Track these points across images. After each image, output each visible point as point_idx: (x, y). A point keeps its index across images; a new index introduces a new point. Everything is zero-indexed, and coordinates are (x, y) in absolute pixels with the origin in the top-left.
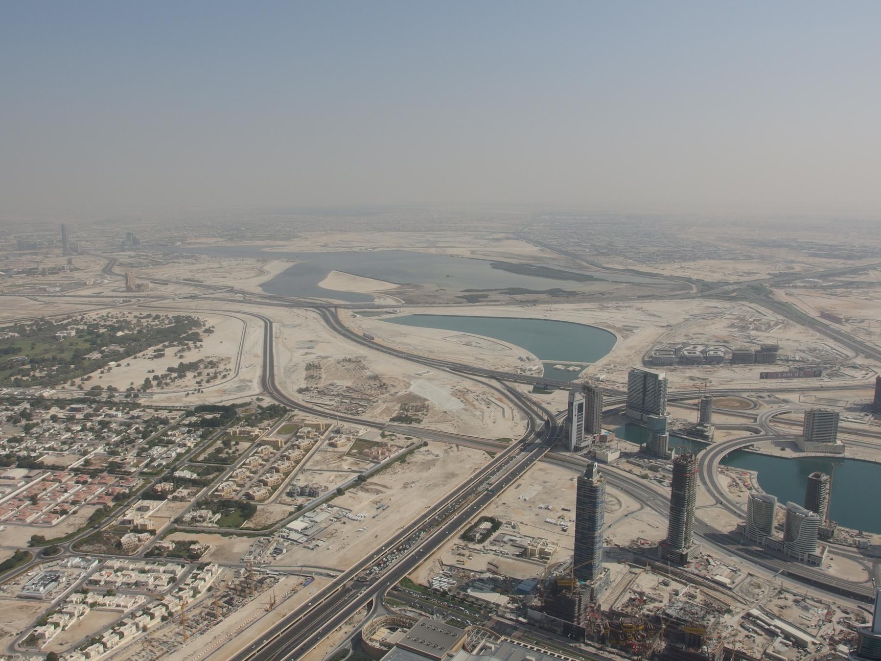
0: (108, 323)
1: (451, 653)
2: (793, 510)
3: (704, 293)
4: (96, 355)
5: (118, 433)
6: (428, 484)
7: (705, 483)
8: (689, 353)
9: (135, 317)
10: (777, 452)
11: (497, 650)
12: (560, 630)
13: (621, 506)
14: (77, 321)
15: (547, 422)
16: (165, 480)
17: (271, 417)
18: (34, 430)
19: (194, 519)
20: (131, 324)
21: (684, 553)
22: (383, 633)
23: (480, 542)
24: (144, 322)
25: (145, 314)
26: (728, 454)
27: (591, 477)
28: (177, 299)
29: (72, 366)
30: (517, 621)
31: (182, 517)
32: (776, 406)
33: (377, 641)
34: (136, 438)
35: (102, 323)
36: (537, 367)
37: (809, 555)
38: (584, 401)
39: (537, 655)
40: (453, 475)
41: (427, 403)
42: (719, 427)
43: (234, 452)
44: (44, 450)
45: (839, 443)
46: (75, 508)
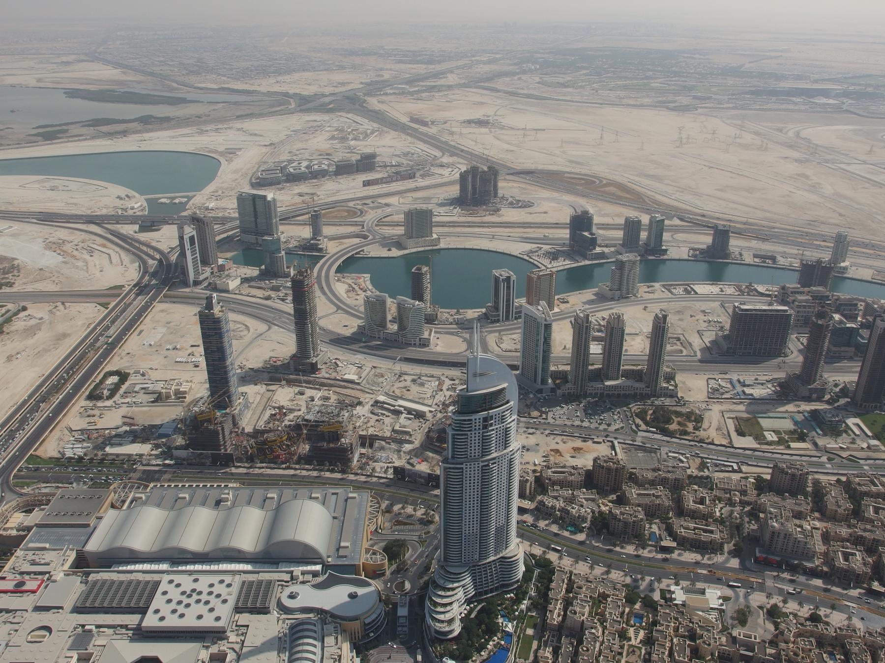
1: (99, 515)
2: (402, 303)
3: (303, 107)
6: (36, 351)
7: (324, 293)
8: (294, 170)
10: (384, 253)
11: (148, 498)
12: (208, 462)
13: (249, 331)
15: (160, 261)
21: (314, 362)
22: (18, 519)
23: (110, 397)
26: (343, 262)
27: (212, 309)
30: (165, 465)
32: (379, 211)
33: (12, 528)
36: (139, 204)
37: (420, 339)
38: (194, 233)
39: (190, 490)
40: (65, 336)
41: (16, 262)
42: (332, 238)
45: (435, 236)
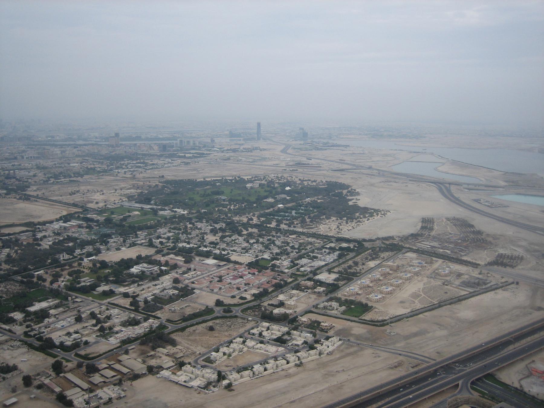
0: (280, 182)
4: (271, 200)
5: (279, 247)
9: (300, 180)
14: (260, 179)
16: (310, 279)
17: (392, 250)
18: (225, 239)
19: (325, 308)
20: (297, 184)
24: (306, 183)
25: (307, 179)
28: (330, 171)
29: (255, 205)
31: (317, 305)
34: (292, 252)
35: (277, 181)
43: (360, 270)
44: (231, 251)
46: (246, 288)
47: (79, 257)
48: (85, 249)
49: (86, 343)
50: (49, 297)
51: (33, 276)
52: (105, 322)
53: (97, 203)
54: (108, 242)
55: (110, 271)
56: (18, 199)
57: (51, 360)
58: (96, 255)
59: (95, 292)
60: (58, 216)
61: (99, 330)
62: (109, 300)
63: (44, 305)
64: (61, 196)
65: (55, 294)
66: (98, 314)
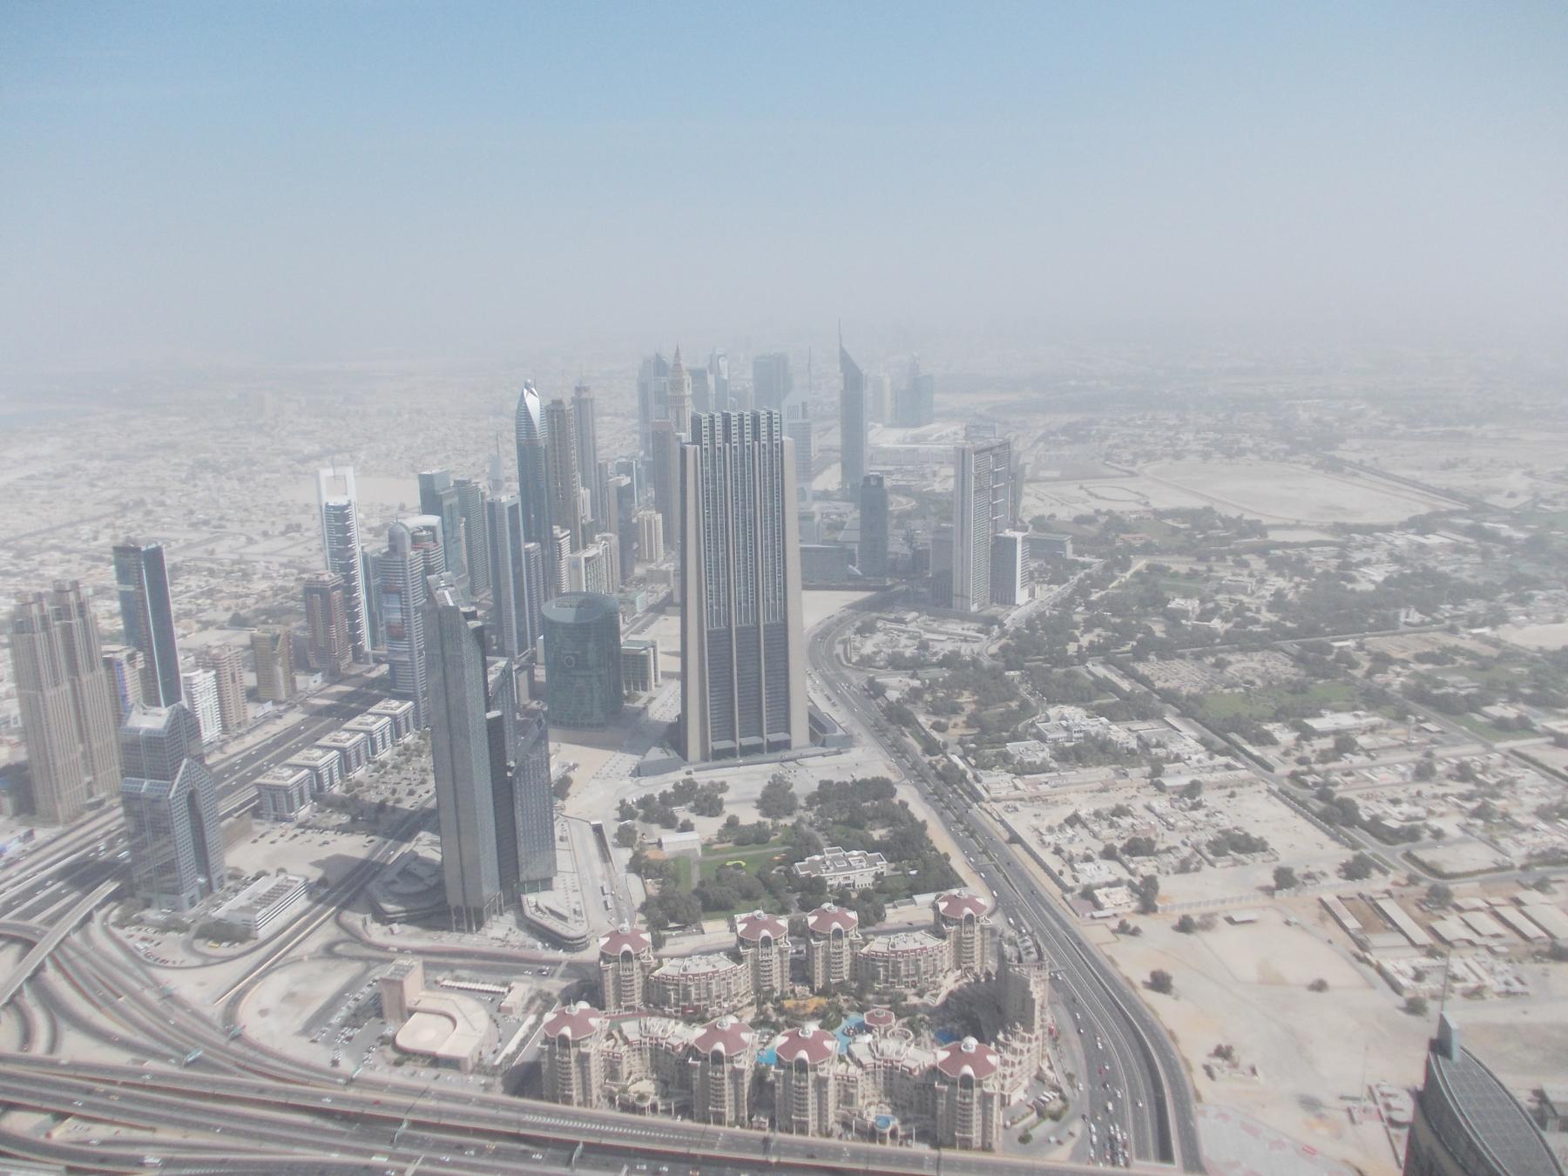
47: (1448, 622)
48: (1464, 604)
49: (1438, 834)
50: (1363, 706)
51: (1330, 649)
52: (1496, 796)
53: (1512, 495)
54: (1531, 597)
55: (1526, 670)
56: (1316, 467)
57: (1347, 855)
58: (1494, 625)
59: (1476, 717)
60: (1405, 517)
61: (1476, 814)
62: (1512, 744)
63: (1345, 720)
64: (1419, 468)
65: (1374, 699)
66: (1480, 773)
